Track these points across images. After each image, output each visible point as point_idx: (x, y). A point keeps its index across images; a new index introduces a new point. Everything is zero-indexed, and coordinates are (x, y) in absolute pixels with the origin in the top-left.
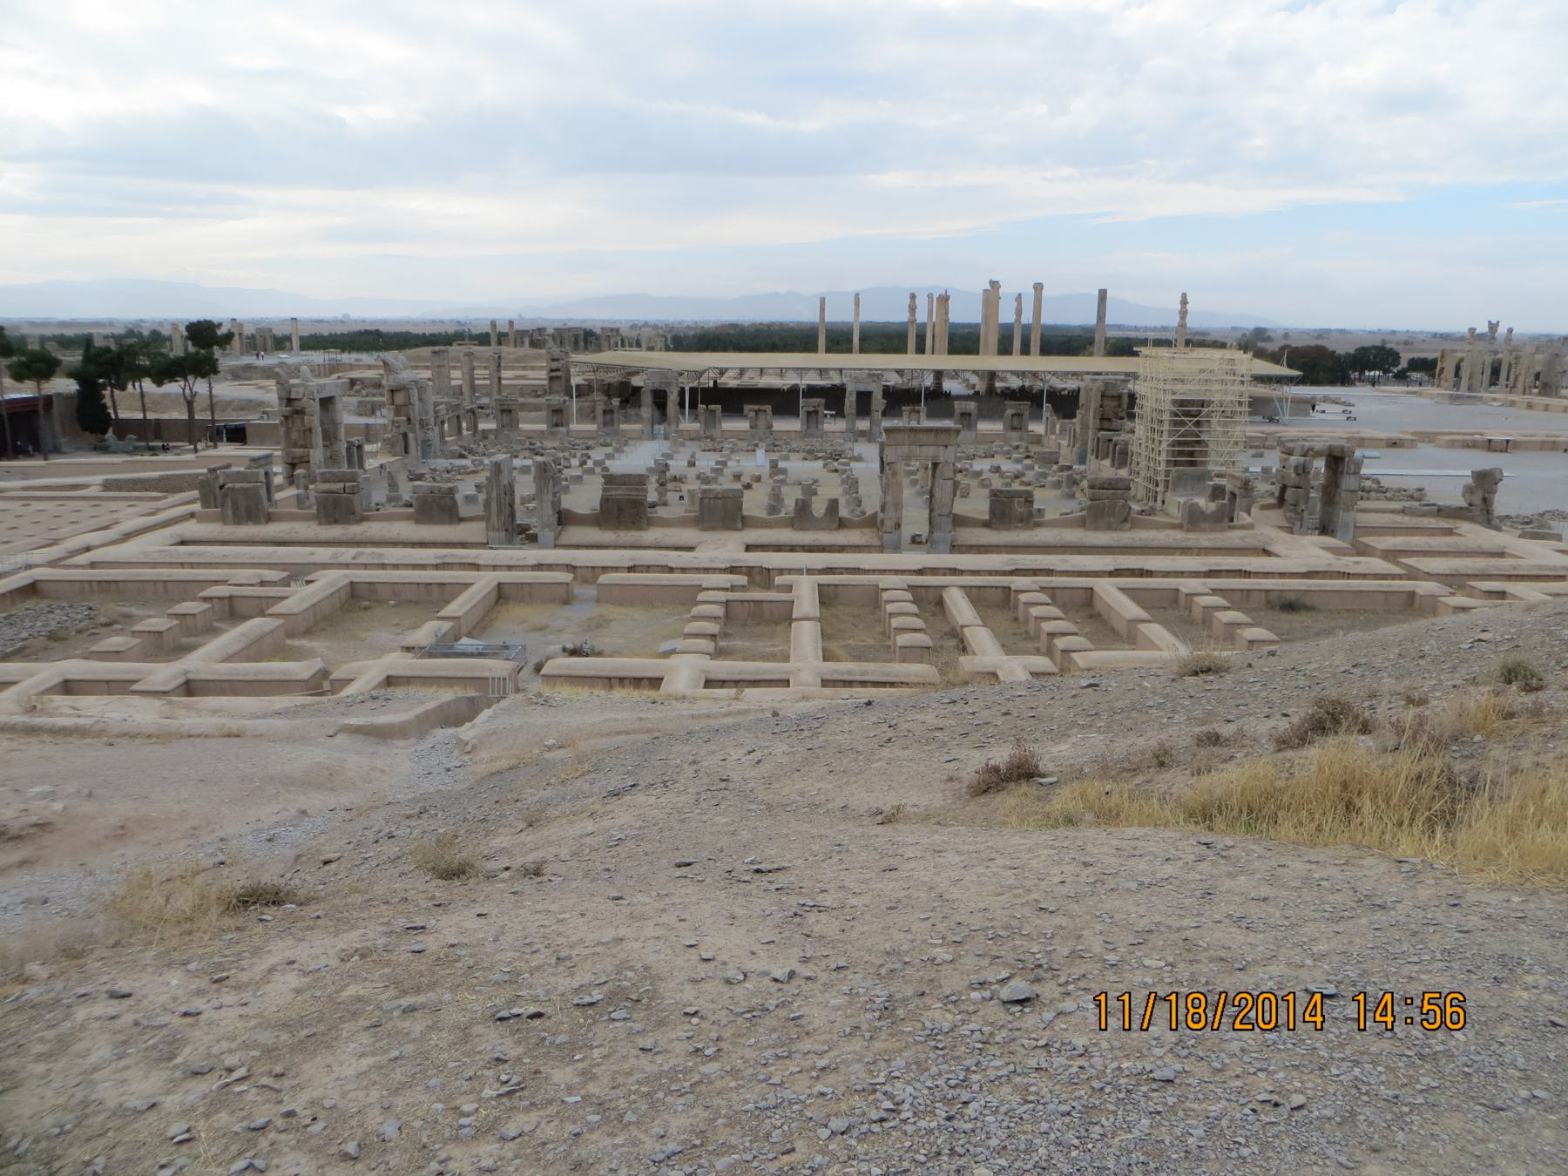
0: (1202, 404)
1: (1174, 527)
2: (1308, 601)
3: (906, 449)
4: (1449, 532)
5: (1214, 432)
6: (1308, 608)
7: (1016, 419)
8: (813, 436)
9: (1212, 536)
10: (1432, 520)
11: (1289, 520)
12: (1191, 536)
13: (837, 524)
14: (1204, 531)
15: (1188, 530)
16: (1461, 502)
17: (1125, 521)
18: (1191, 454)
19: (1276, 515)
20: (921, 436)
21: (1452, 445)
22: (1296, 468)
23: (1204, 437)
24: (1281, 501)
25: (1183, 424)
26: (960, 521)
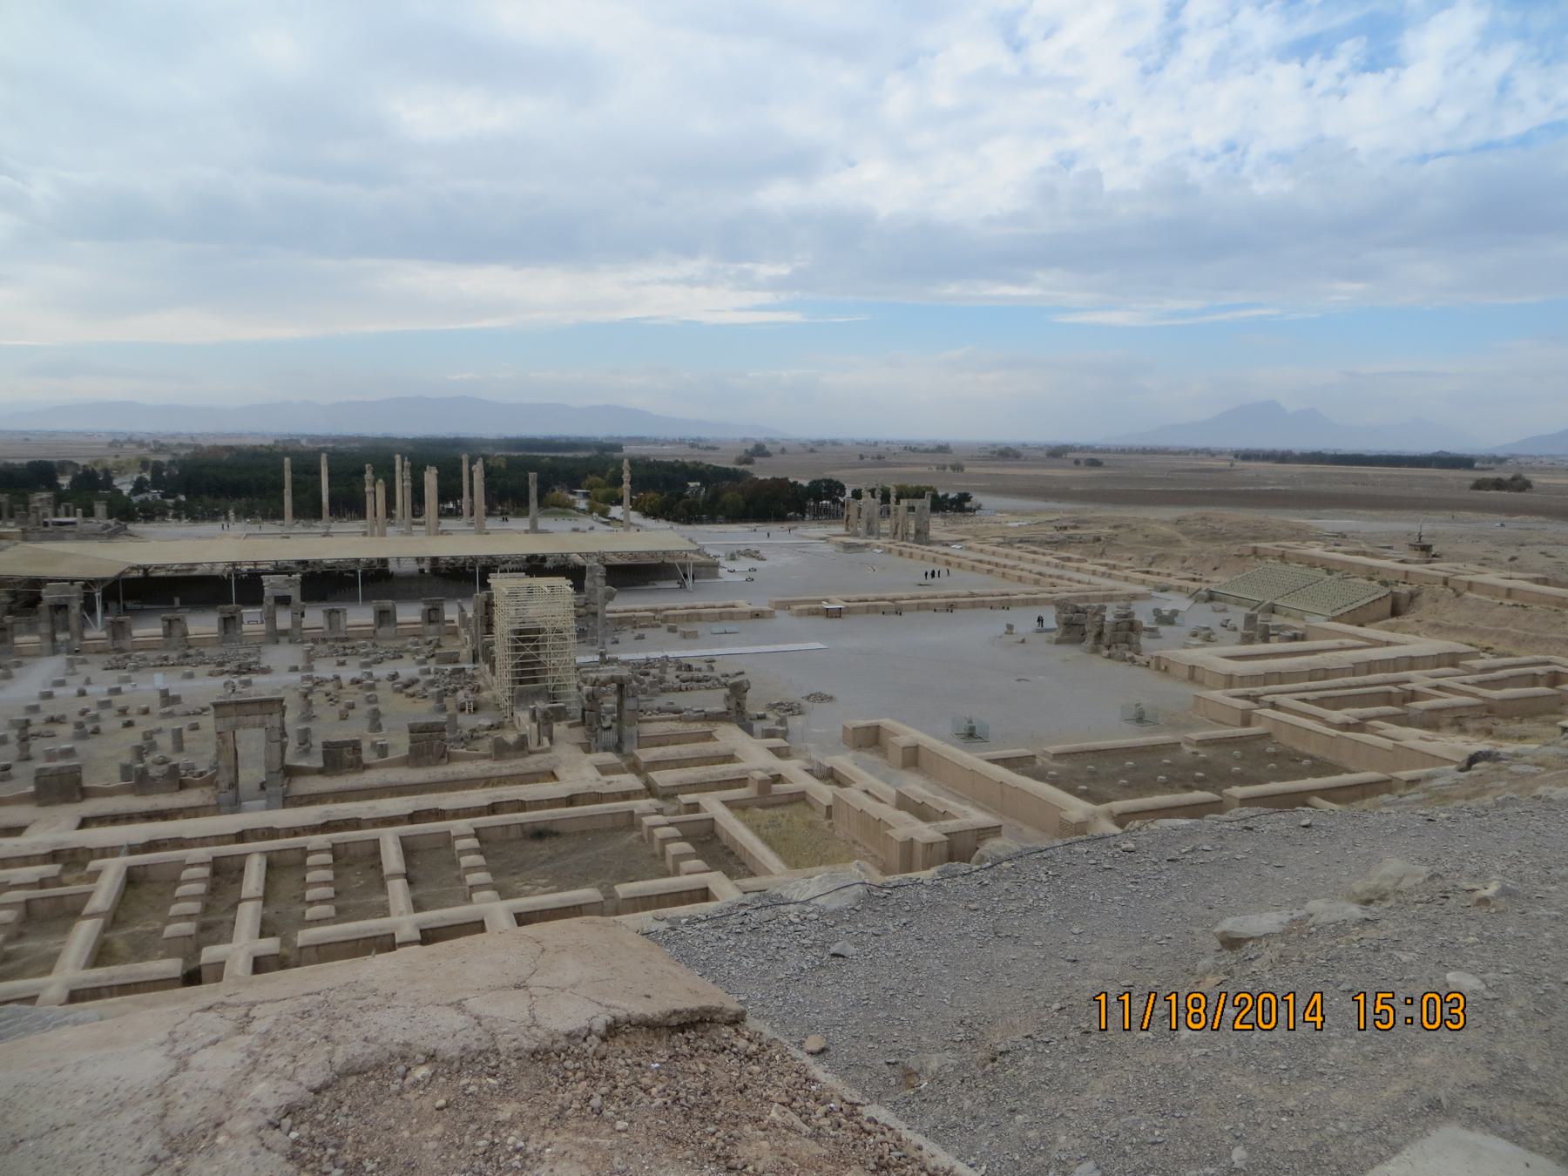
0: (539, 631)
1: (485, 757)
2: (555, 828)
3: (234, 719)
4: (708, 737)
5: (549, 658)
6: (557, 834)
7: (432, 613)
8: (231, 641)
9: (514, 762)
10: (699, 725)
11: (587, 737)
12: (497, 765)
13: (177, 787)
14: (510, 758)
15: (495, 760)
16: (721, 708)
17: (442, 757)
18: (533, 672)
19: (579, 734)
20: (248, 708)
21: (800, 613)
22: (587, 696)
23: (542, 659)
24: (583, 722)
25: (522, 648)
26: (290, 772)
